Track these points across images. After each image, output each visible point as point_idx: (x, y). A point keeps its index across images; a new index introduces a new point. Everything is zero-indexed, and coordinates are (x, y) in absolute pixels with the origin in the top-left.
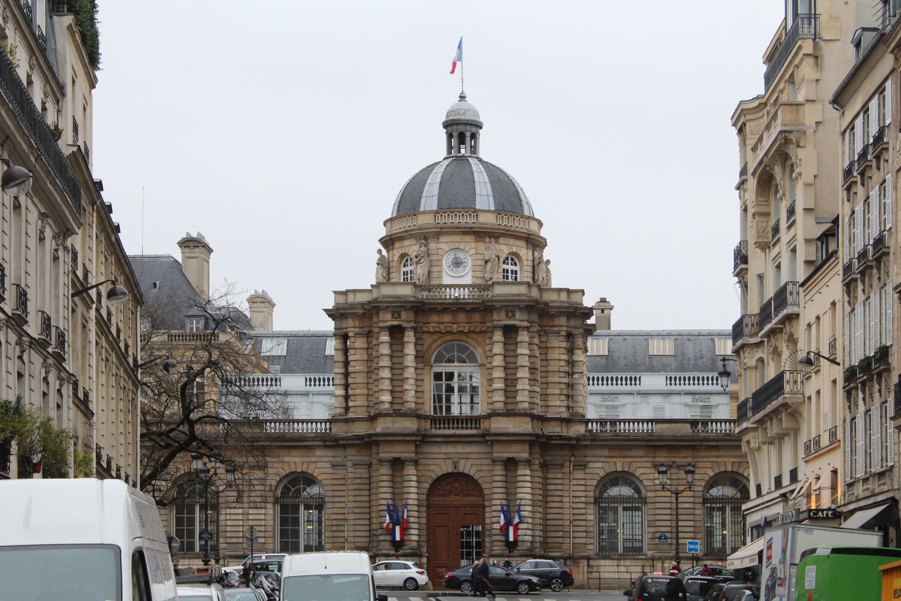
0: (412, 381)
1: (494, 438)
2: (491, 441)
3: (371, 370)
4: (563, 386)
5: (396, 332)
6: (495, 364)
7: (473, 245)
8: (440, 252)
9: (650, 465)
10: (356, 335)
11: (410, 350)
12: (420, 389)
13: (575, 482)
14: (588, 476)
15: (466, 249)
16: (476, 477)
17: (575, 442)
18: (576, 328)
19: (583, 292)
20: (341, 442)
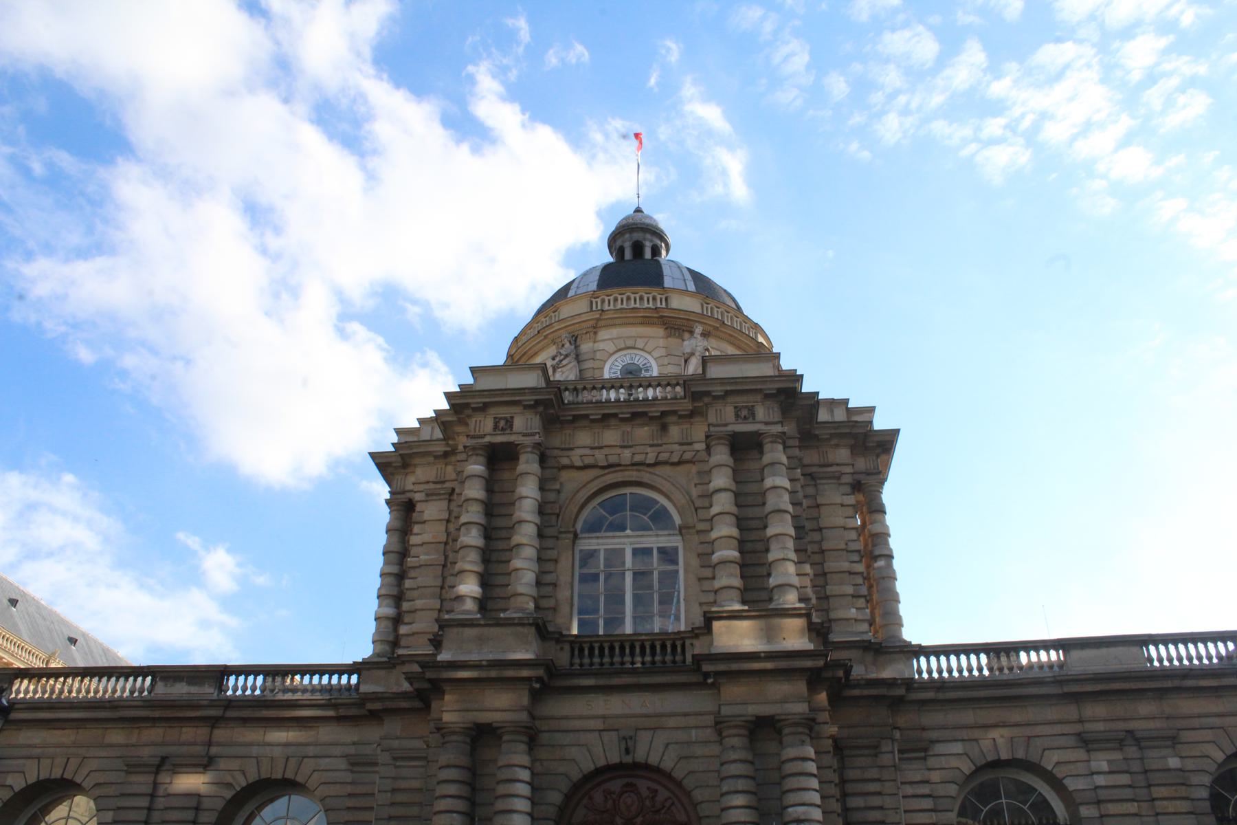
0: (530, 552)
1: (722, 667)
2: (718, 674)
3: (449, 545)
4: (860, 580)
5: (500, 458)
6: (715, 510)
7: (661, 342)
8: (598, 356)
9: (1071, 741)
10: (430, 495)
11: (528, 490)
12: (548, 578)
13: (909, 790)
14: (935, 776)
15: (647, 348)
16: (678, 774)
17: (901, 692)
18: (869, 474)
19: (871, 410)
20: (370, 706)
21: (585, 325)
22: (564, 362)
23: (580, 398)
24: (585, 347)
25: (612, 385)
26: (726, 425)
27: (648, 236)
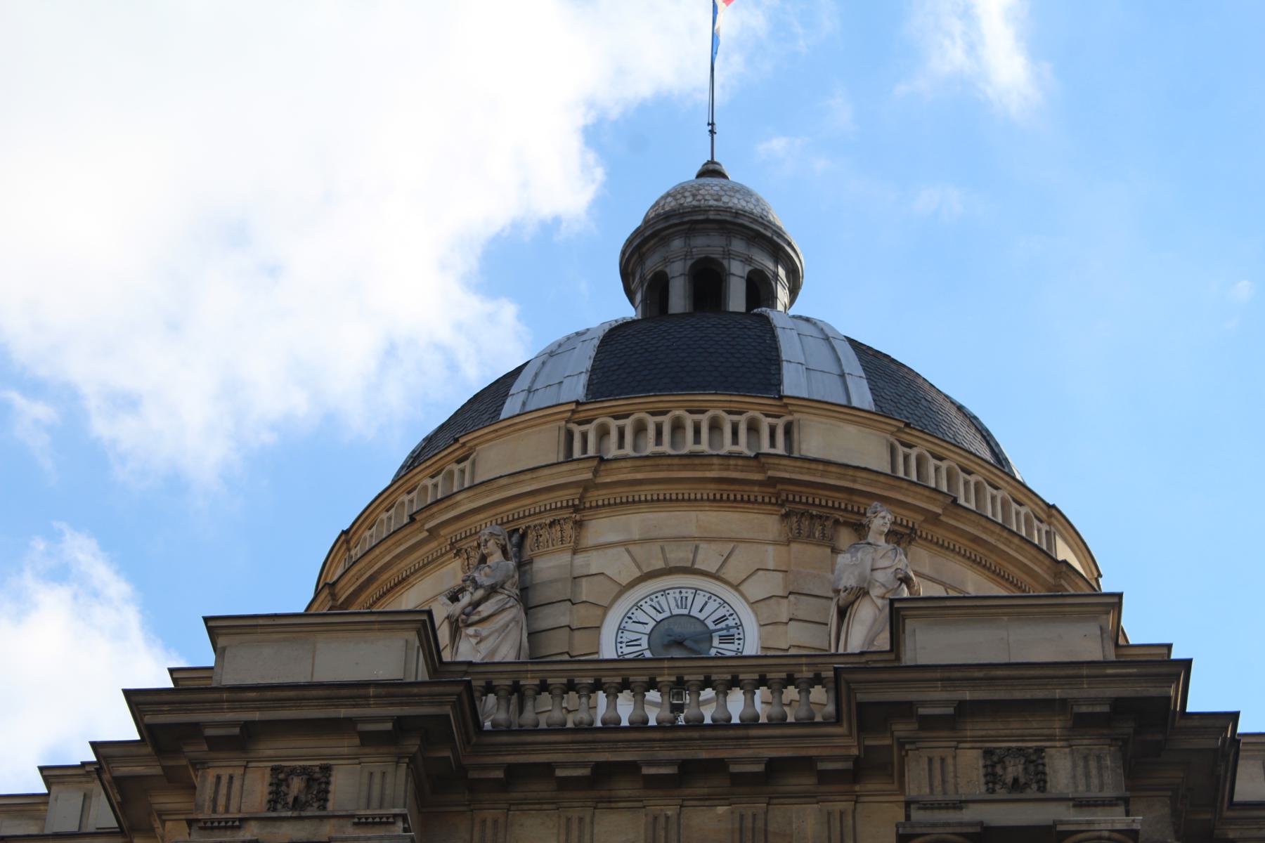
7: (771, 555)
8: (586, 591)
15: (730, 573)
21: (544, 501)
22: (486, 609)
23: (529, 716)
24: (550, 565)
25: (625, 677)
26: (959, 805)
27: (738, 246)
